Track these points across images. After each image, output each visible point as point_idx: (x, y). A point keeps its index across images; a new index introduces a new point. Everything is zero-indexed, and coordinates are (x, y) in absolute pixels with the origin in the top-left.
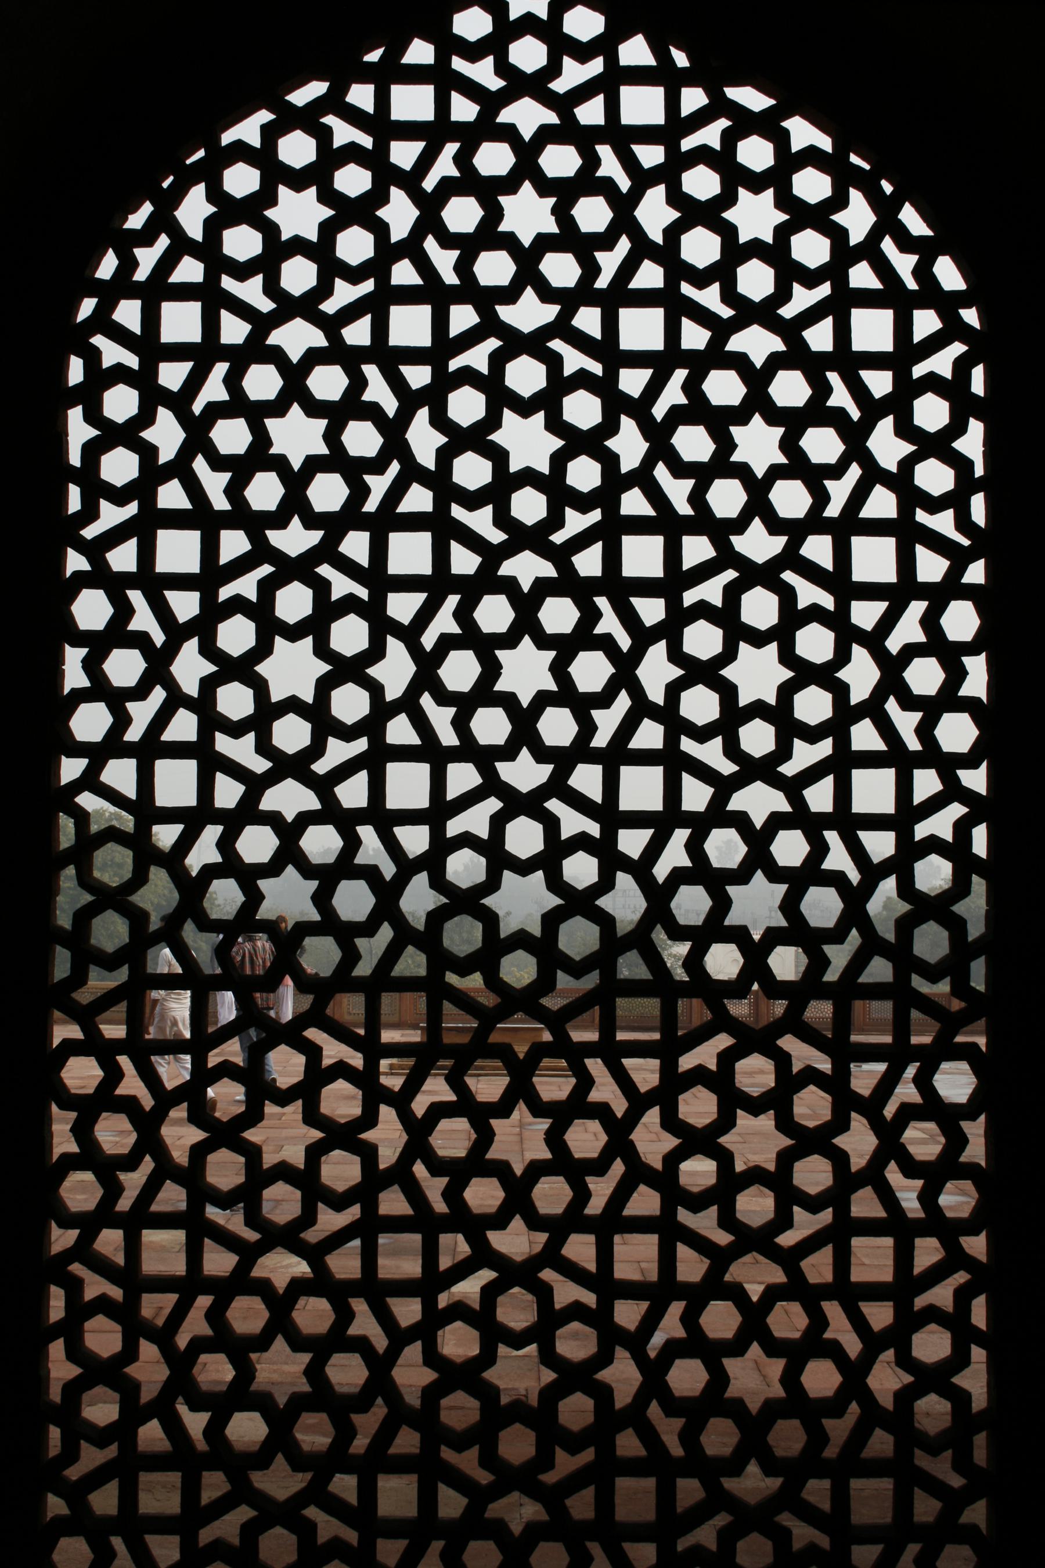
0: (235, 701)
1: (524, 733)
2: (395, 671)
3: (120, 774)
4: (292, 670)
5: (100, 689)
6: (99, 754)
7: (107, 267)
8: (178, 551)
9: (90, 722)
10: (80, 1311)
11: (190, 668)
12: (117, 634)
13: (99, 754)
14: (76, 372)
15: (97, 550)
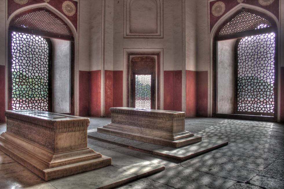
0: (247, 65)
1: (262, 65)
2: (255, 63)
3: (241, 69)
4: (250, 63)
5: (240, 65)
6: (240, 68)
7: (240, 43)
8: (244, 58)
9: (239, 67)
10: (239, 96)
11: (244, 64)
12: (241, 62)
13: (240, 68)
14: (238, 49)
15: (240, 58)
